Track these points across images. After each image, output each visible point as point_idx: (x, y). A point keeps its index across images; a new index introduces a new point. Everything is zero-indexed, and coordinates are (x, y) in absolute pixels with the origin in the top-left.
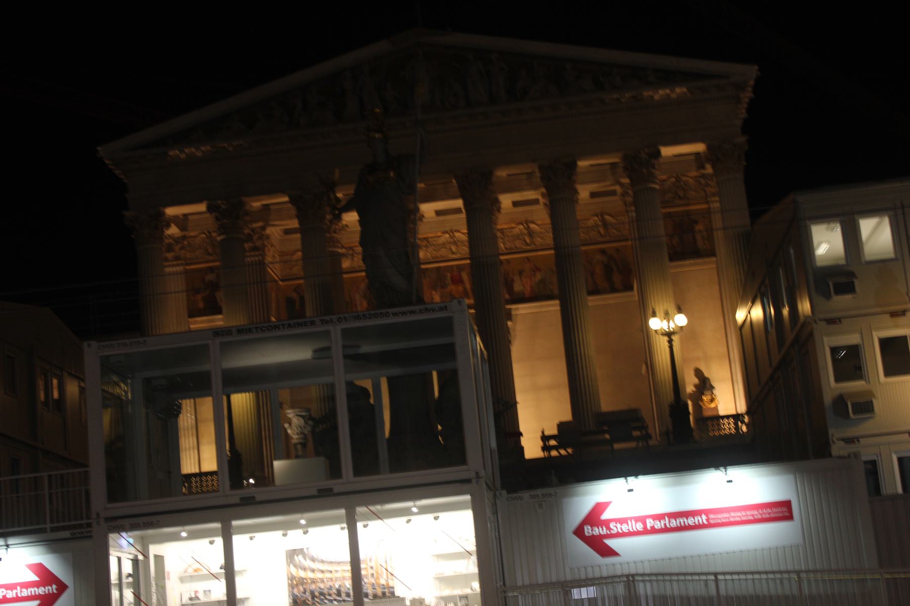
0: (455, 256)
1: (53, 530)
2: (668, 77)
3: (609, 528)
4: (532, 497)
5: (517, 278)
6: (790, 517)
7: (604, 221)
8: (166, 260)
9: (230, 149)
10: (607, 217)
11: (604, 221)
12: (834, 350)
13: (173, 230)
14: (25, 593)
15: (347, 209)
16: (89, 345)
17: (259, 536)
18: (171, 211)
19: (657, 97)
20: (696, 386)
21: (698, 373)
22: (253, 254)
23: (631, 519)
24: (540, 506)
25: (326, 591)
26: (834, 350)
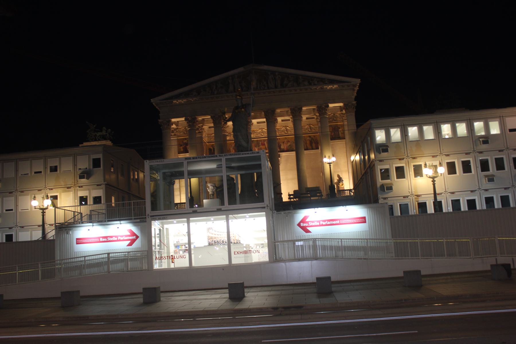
0: (263, 137)
1: (134, 219)
2: (332, 82)
3: (308, 224)
4: (284, 213)
5: (282, 144)
6: (365, 222)
7: (310, 127)
8: (172, 136)
9: (193, 101)
10: (311, 126)
11: (310, 127)
12: (381, 170)
13: (174, 126)
14: (126, 238)
15: (229, 121)
16: (146, 161)
17: (198, 223)
18: (173, 120)
19: (328, 88)
20: (337, 180)
21: (338, 176)
22: (199, 134)
23: (315, 221)
24: (287, 216)
25: (219, 241)
26: (381, 170)
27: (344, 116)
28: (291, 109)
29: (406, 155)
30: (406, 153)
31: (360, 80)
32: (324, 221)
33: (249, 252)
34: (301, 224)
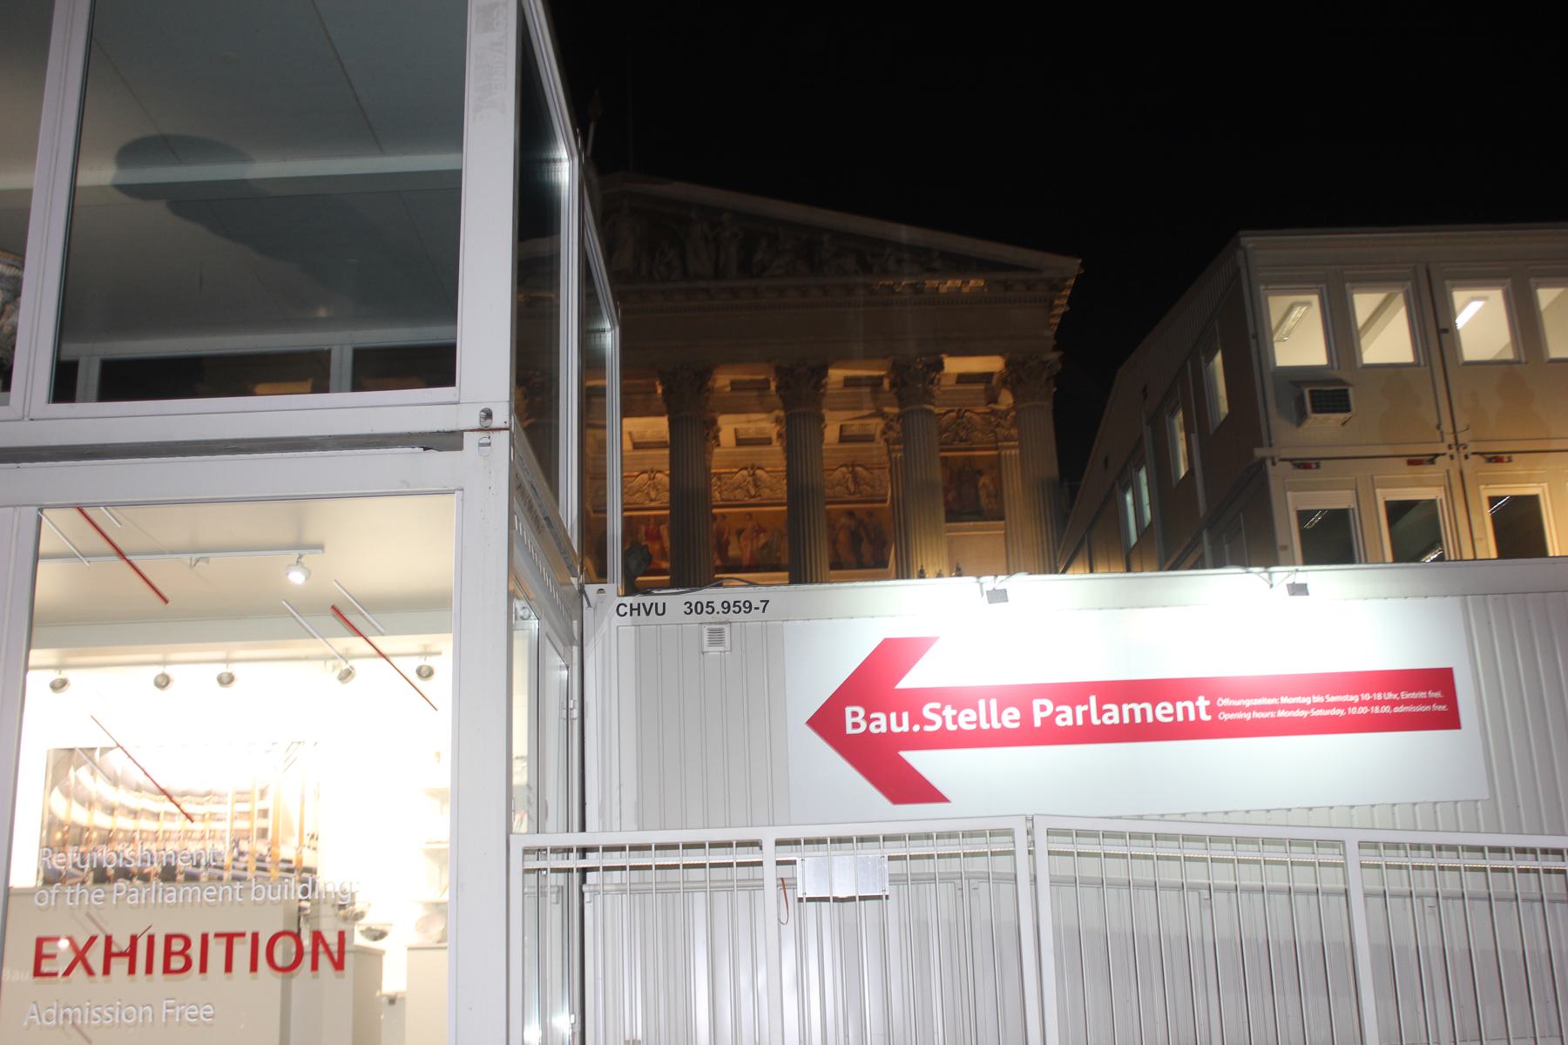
2: (961, 265)
3: (917, 718)
4: (693, 609)
6: (1450, 720)
7: (854, 473)
10: (859, 469)
11: (854, 473)
12: (1304, 516)
19: (943, 289)
23: (987, 693)
24: (716, 636)
26: (1304, 516)
27: (1002, 422)
28: (778, 370)
29: (1449, 439)
30: (1447, 427)
31: (1080, 261)
32: (1073, 693)
33: (217, 950)
34: (849, 720)
